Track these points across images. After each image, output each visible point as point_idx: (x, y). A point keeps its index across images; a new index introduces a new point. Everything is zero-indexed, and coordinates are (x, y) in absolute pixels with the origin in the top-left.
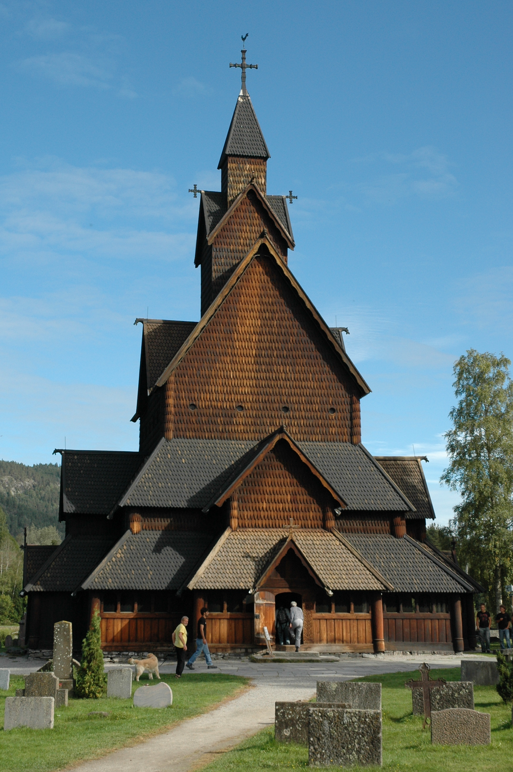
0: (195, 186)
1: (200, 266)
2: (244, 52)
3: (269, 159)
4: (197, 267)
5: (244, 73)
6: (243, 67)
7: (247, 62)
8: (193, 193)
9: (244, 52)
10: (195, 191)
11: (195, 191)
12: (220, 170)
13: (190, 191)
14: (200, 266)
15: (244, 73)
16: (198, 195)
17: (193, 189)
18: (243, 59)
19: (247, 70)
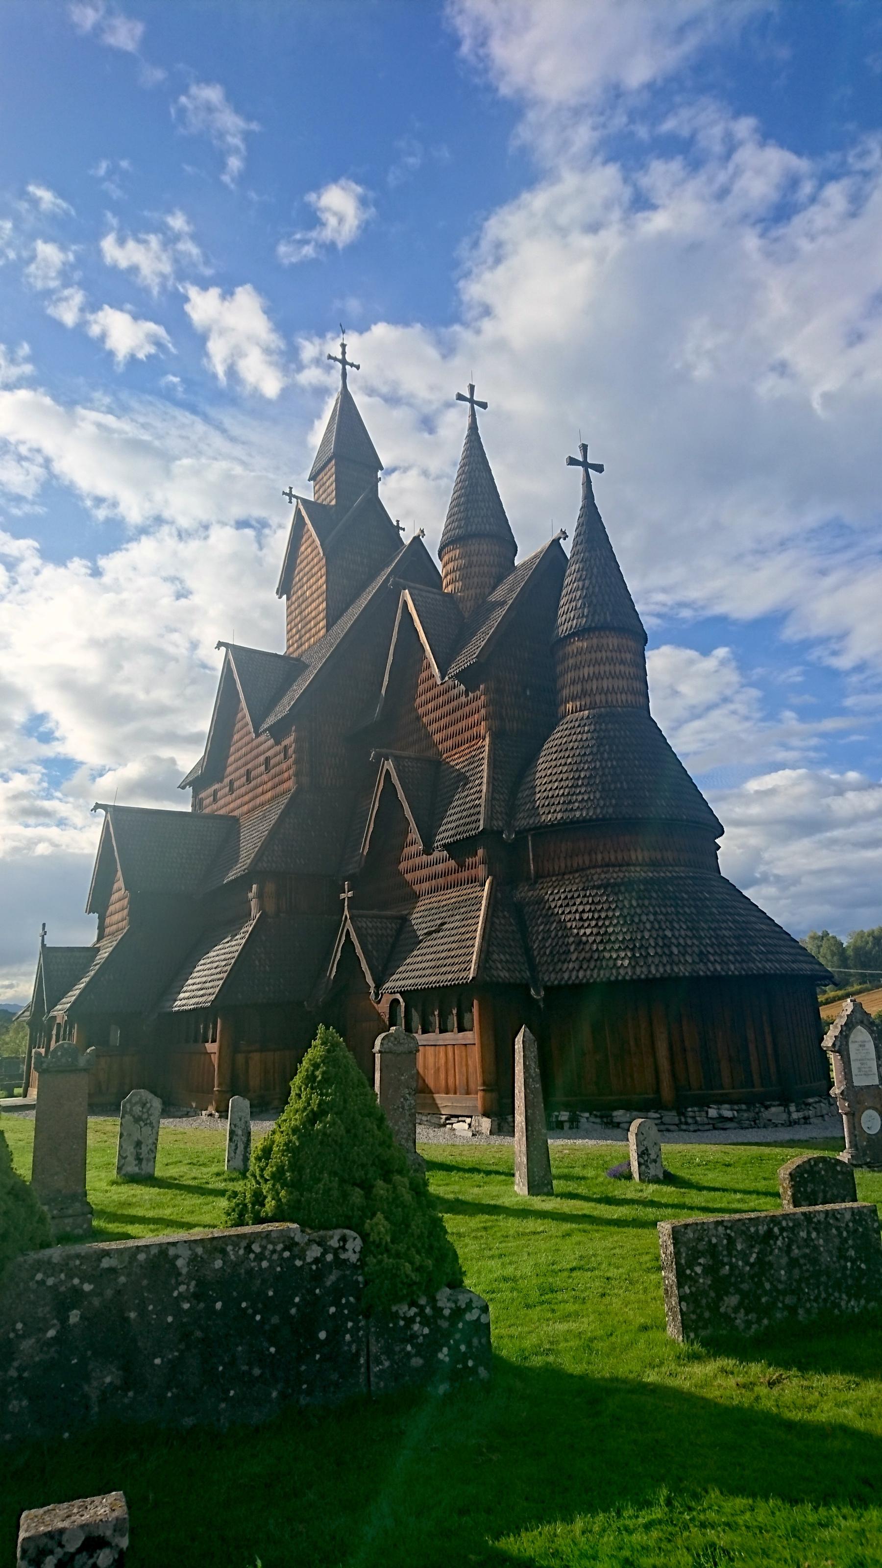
0: (291, 488)
1: (285, 597)
4: (280, 598)
5: (344, 369)
7: (348, 358)
10: (290, 495)
11: (290, 495)
12: (312, 482)
14: (285, 597)
15: (344, 369)
17: (287, 491)
18: (344, 353)
19: (348, 367)
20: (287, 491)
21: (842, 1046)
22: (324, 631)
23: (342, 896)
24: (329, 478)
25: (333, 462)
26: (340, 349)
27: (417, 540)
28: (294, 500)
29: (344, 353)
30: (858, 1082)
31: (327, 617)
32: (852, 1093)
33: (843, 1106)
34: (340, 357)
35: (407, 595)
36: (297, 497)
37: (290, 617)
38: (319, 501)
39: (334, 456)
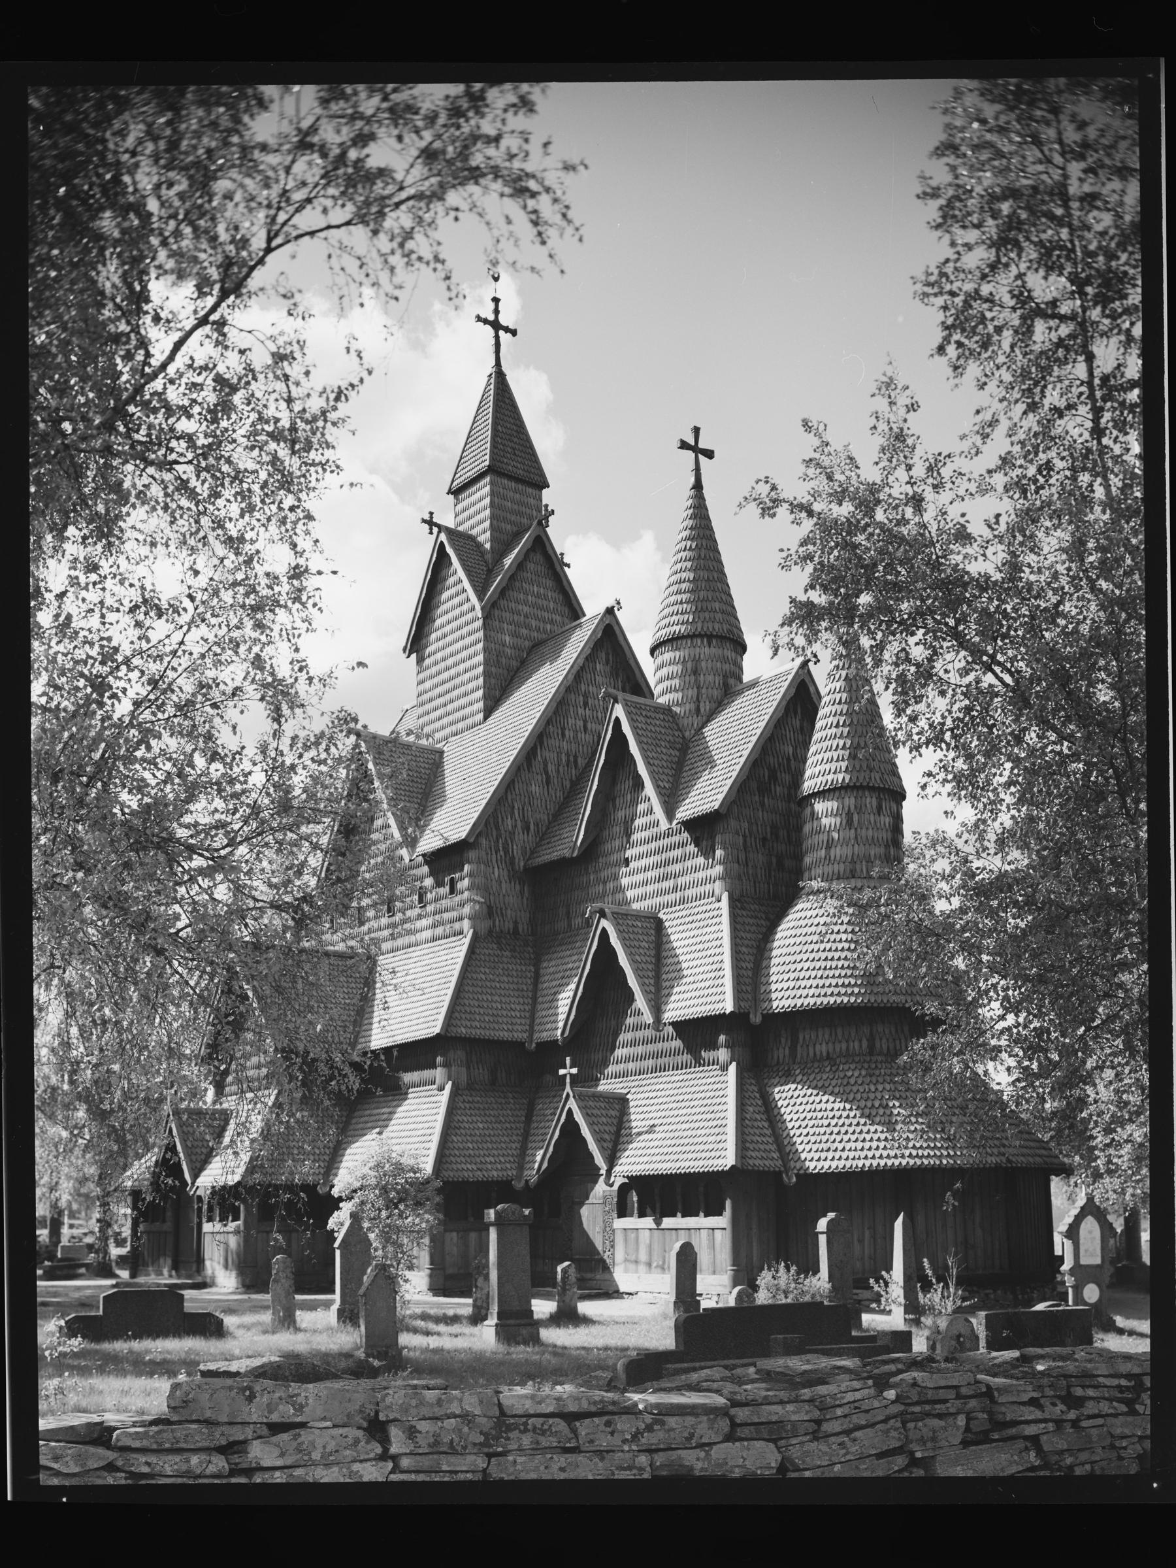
1: (414, 656)
2: (496, 300)
3: (545, 491)
5: (497, 337)
6: (496, 325)
7: (504, 320)
8: (427, 527)
9: (496, 300)
10: (430, 523)
13: (424, 521)
14: (414, 656)
15: (497, 337)
16: (435, 530)
17: (427, 517)
18: (496, 312)
19: (501, 333)
20: (427, 517)
21: (1072, 1232)
22: (481, 716)
23: (562, 1072)
24: (482, 493)
25: (488, 479)
26: (492, 306)
27: (610, 611)
28: (435, 530)
29: (496, 312)
30: (1083, 1261)
31: (485, 697)
32: (1077, 1269)
33: (1069, 1281)
34: (491, 317)
35: (619, 711)
36: (439, 526)
37: (421, 687)
38: (461, 528)
39: (490, 470)
